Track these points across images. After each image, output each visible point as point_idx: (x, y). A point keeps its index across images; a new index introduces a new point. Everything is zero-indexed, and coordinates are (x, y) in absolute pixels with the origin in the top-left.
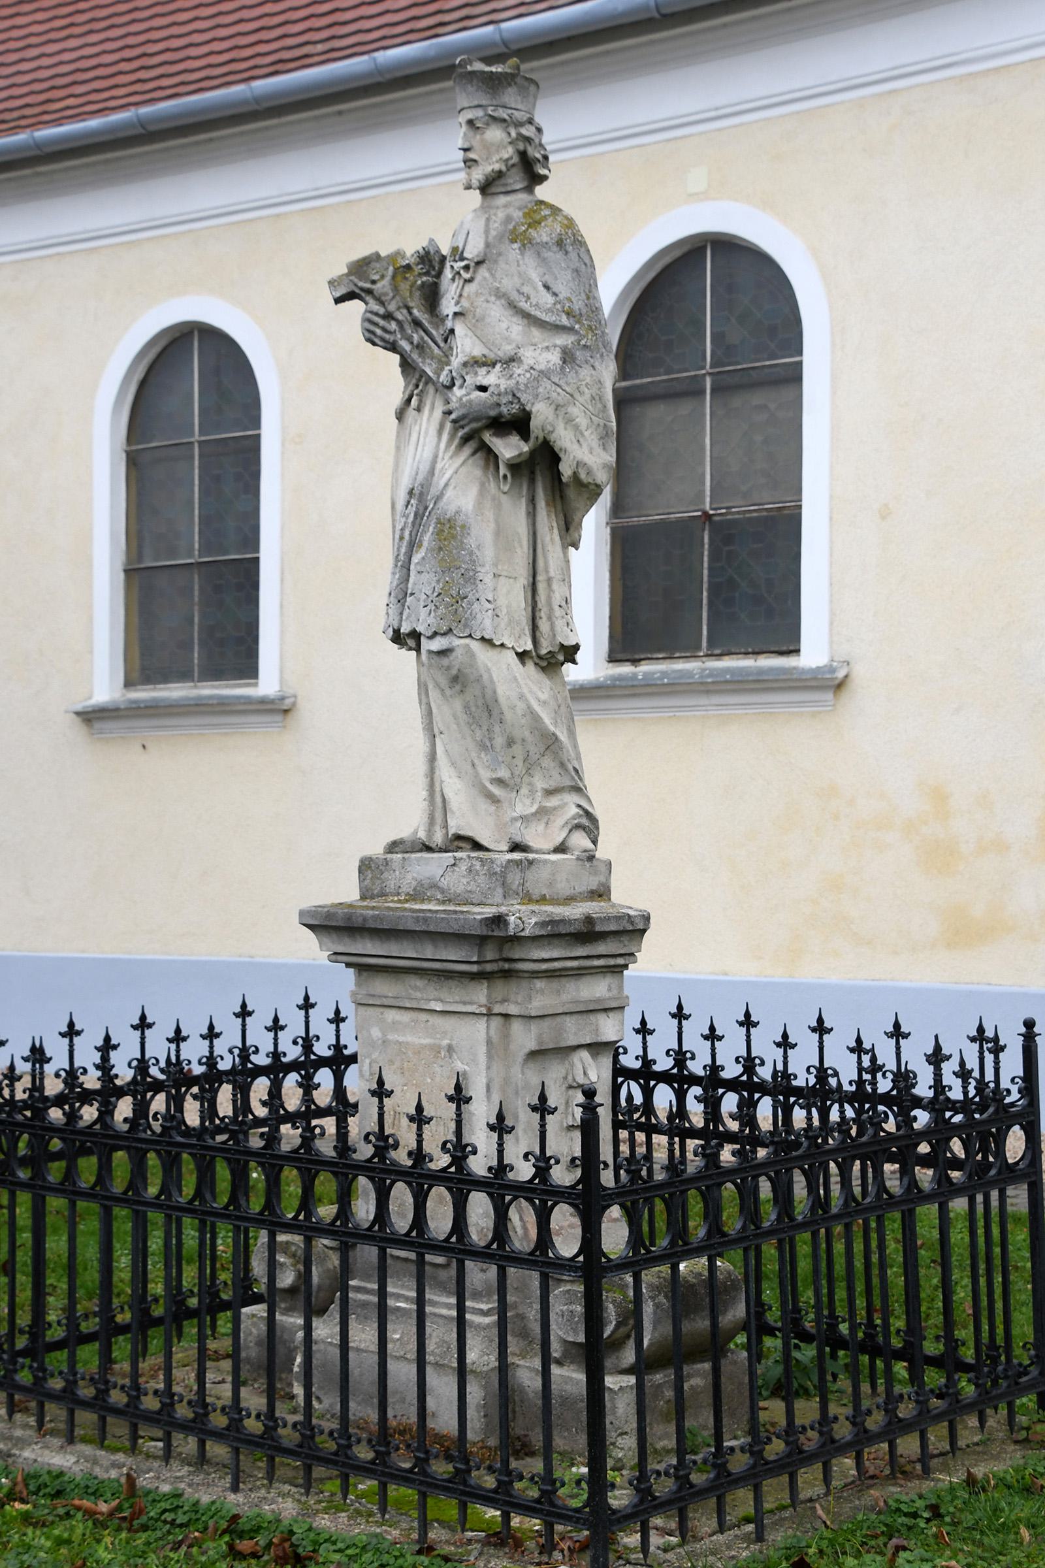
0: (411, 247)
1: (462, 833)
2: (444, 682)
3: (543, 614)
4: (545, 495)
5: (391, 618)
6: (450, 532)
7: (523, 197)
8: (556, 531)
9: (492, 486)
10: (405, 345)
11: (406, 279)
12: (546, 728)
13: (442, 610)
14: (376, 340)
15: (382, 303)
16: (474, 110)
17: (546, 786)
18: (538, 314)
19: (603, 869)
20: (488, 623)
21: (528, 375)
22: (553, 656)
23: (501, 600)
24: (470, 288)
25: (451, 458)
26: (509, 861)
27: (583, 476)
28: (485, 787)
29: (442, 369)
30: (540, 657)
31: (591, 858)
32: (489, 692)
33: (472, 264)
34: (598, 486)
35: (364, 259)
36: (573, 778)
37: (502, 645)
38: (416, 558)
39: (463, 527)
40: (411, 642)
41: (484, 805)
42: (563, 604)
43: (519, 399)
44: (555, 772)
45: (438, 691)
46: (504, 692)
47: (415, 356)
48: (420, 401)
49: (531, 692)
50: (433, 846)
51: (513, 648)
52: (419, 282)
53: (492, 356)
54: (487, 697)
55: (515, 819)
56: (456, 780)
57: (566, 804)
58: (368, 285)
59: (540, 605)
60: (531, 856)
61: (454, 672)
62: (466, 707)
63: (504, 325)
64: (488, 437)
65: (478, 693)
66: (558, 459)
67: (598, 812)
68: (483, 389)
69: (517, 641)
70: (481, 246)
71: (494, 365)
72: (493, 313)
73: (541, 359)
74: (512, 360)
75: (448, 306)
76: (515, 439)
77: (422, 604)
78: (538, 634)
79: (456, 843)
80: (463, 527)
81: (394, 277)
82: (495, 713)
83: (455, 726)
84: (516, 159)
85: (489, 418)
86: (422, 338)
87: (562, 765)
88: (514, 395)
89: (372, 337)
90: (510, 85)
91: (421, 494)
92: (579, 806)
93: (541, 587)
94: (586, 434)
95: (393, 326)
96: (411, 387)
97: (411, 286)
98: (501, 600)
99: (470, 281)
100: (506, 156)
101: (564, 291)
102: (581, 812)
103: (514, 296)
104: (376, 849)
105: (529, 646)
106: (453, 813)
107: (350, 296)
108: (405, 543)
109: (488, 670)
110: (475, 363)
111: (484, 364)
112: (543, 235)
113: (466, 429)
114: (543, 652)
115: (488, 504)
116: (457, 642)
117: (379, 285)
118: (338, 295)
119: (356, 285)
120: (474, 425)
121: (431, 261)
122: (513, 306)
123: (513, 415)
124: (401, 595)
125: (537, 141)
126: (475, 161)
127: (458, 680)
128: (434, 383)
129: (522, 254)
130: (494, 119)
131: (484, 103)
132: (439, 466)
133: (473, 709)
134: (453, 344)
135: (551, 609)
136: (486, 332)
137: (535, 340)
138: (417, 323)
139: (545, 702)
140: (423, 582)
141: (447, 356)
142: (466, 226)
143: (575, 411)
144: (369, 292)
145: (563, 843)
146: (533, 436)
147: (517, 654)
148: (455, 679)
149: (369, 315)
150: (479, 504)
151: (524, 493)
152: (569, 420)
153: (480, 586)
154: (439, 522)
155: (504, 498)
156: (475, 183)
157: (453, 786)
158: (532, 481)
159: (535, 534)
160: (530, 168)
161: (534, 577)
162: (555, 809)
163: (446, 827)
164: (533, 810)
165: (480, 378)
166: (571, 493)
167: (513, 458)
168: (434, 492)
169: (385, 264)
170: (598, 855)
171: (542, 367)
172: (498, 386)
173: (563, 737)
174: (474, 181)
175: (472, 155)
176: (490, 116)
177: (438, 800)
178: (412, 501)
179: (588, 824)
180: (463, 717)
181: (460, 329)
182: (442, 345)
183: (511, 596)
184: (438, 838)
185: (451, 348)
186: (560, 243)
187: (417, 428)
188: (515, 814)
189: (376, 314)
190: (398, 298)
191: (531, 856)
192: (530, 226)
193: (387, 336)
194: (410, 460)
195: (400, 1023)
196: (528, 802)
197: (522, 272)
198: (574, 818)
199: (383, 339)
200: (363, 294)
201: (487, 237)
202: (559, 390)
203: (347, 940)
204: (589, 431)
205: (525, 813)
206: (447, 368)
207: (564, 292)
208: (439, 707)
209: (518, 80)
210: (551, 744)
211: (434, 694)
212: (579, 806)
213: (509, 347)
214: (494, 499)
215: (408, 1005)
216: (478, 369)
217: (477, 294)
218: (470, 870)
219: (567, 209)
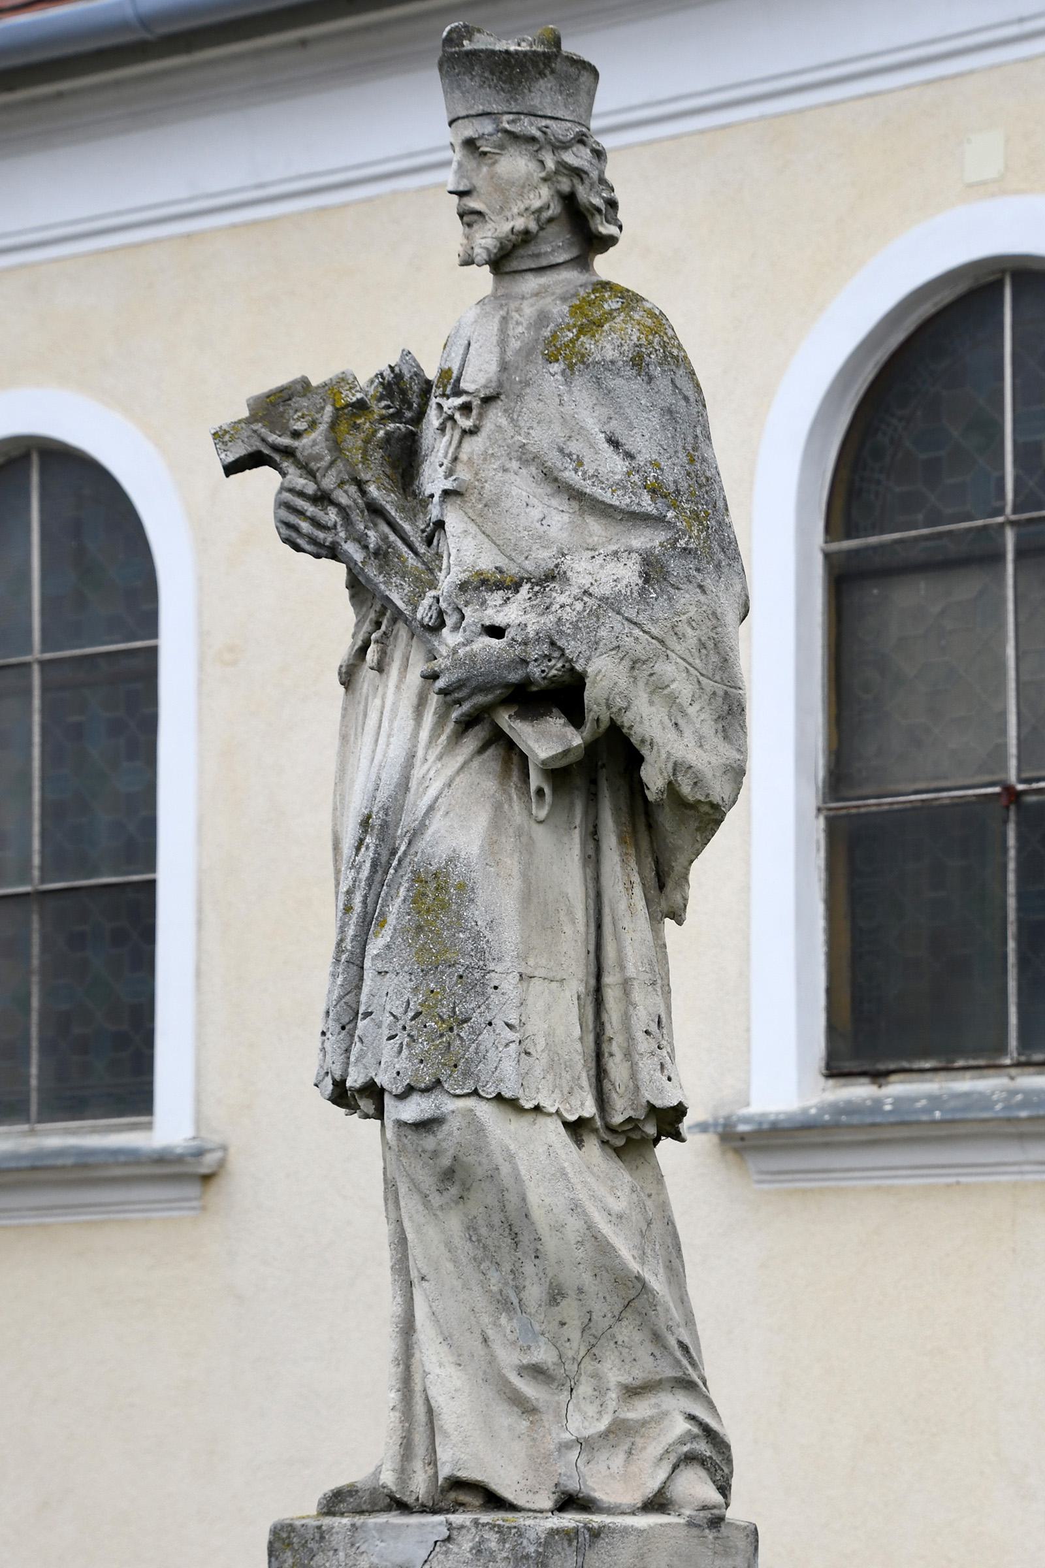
0: (366, 367)
1: (463, 1474)
2: (427, 1181)
3: (615, 1048)
4: (617, 823)
5: (329, 1059)
6: (438, 896)
7: (571, 277)
8: (638, 891)
9: (516, 810)
10: (352, 549)
11: (357, 427)
12: (624, 1267)
13: (422, 1045)
14: (301, 542)
15: (311, 474)
16: (476, 122)
17: (626, 1379)
18: (597, 492)
19: (742, 1543)
20: (508, 1067)
21: (579, 606)
22: (636, 1128)
23: (534, 1023)
24: (473, 446)
25: (440, 758)
26: (553, 1532)
27: (686, 789)
28: (507, 1382)
29: (421, 596)
30: (611, 1129)
31: (716, 1522)
32: (512, 1198)
33: (476, 402)
34: (715, 807)
35: (281, 390)
36: (678, 1362)
37: (537, 1109)
38: (373, 948)
39: (461, 887)
40: (366, 1105)
41: (507, 1419)
42: (653, 1028)
43: (562, 650)
44: (643, 1352)
45: (416, 1197)
46: (542, 1199)
47: (371, 571)
48: (383, 654)
49: (593, 1197)
50: (410, 1500)
51: (557, 1112)
52: (381, 433)
53: (513, 570)
54: (510, 1207)
55: (565, 1446)
56: (452, 1370)
57: (665, 1414)
58: (285, 441)
59: (609, 1032)
60: (596, 1520)
61: (446, 1162)
62: (471, 1228)
63: (536, 513)
64: (505, 720)
65: (491, 1200)
66: (639, 759)
67: (730, 1430)
68: (496, 632)
69: (565, 1100)
70: (493, 368)
71: (516, 587)
72: (515, 491)
73: (603, 575)
74: (551, 577)
75: (433, 480)
76: (556, 724)
77: (386, 1033)
78: (607, 1085)
79: (452, 1495)
80: (461, 887)
81: (333, 425)
82: (525, 1239)
83: (450, 1266)
84: (555, 209)
85: (508, 685)
86: (385, 538)
87: (657, 1337)
88: (553, 644)
89: (294, 535)
90: (542, 74)
91: (385, 825)
92: (692, 1418)
93: (612, 996)
94: (692, 710)
95: (332, 516)
96: (367, 626)
97: (367, 442)
98: (534, 1023)
99: (473, 432)
100: (537, 204)
101: (645, 446)
102: (696, 1430)
103: (553, 459)
104: (302, 1507)
105: (589, 1109)
106: (446, 1435)
107: (253, 460)
108: (354, 917)
109: (511, 1158)
110: (482, 584)
111: (499, 586)
112: (606, 347)
113: (466, 707)
114: (617, 1119)
115: (508, 843)
116: (450, 1105)
117: (305, 441)
118: (231, 458)
119: (263, 440)
120: (480, 699)
121: (405, 393)
122: (550, 477)
123: (552, 680)
124: (348, 1016)
125: (594, 175)
127: (454, 1177)
128: (406, 621)
129: (568, 383)
130: (514, 137)
131: (495, 108)
132: (417, 773)
133: (484, 1231)
134: (443, 548)
135: (630, 1038)
136: (505, 524)
137: (592, 541)
138: (375, 511)
139: (620, 1217)
140: (388, 992)
141: (431, 571)
142: (466, 332)
143: (667, 669)
144: (288, 452)
145: (661, 1492)
146: (589, 717)
147: (566, 1124)
148: (448, 1176)
149: (287, 496)
150: (491, 845)
151: (578, 821)
152: (658, 688)
153: (495, 998)
154: (416, 878)
155: (539, 832)
156: (480, 254)
157: (447, 1382)
158: (593, 798)
159: (598, 896)
160: (583, 225)
161: (599, 976)
162: (644, 1423)
163: (433, 1462)
164: (602, 1426)
165: (490, 611)
166: (666, 820)
167: (554, 758)
168: (408, 821)
169: (319, 400)
170: (730, 1514)
171: (605, 590)
172: (523, 626)
173: (657, 1283)
174: (477, 250)
175: (473, 204)
176: (506, 131)
177: (420, 1409)
178: (368, 840)
179: (711, 1453)
180: (465, 1249)
181: (454, 521)
182: (422, 549)
183: (553, 1015)
184: (420, 1486)
185: (439, 556)
186: (638, 362)
187: (378, 702)
188: (566, 1436)
189: (301, 494)
190: (340, 464)
191: (596, 1520)
192: (582, 330)
193: (321, 535)
194: (364, 763)
196: (591, 1410)
197: (568, 414)
198: (681, 1441)
199: (313, 541)
200: (277, 457)
201: (503, 352)
202: (637, 632)
204: (696, 707)
205: (586, 1433)
206: (433, 593)
207: (646, 451)
208: (418, 1230)
209: (558, 65)
210: (633, 1296)
211: (410, 1204)
212: (692, 1418)
213: (545, 554)
214: (519, 834)
216: (487, 595)
217: (486, 457)
219: (656, 296)
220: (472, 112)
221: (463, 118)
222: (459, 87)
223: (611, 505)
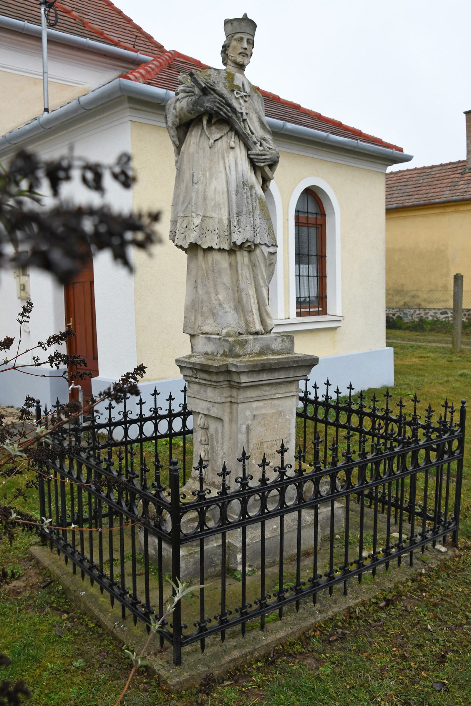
126: (247, 55)
189: (222, 101)
195: (259, 406)
203: (255, 375)
215: (266, 398)
218: (283, 340)
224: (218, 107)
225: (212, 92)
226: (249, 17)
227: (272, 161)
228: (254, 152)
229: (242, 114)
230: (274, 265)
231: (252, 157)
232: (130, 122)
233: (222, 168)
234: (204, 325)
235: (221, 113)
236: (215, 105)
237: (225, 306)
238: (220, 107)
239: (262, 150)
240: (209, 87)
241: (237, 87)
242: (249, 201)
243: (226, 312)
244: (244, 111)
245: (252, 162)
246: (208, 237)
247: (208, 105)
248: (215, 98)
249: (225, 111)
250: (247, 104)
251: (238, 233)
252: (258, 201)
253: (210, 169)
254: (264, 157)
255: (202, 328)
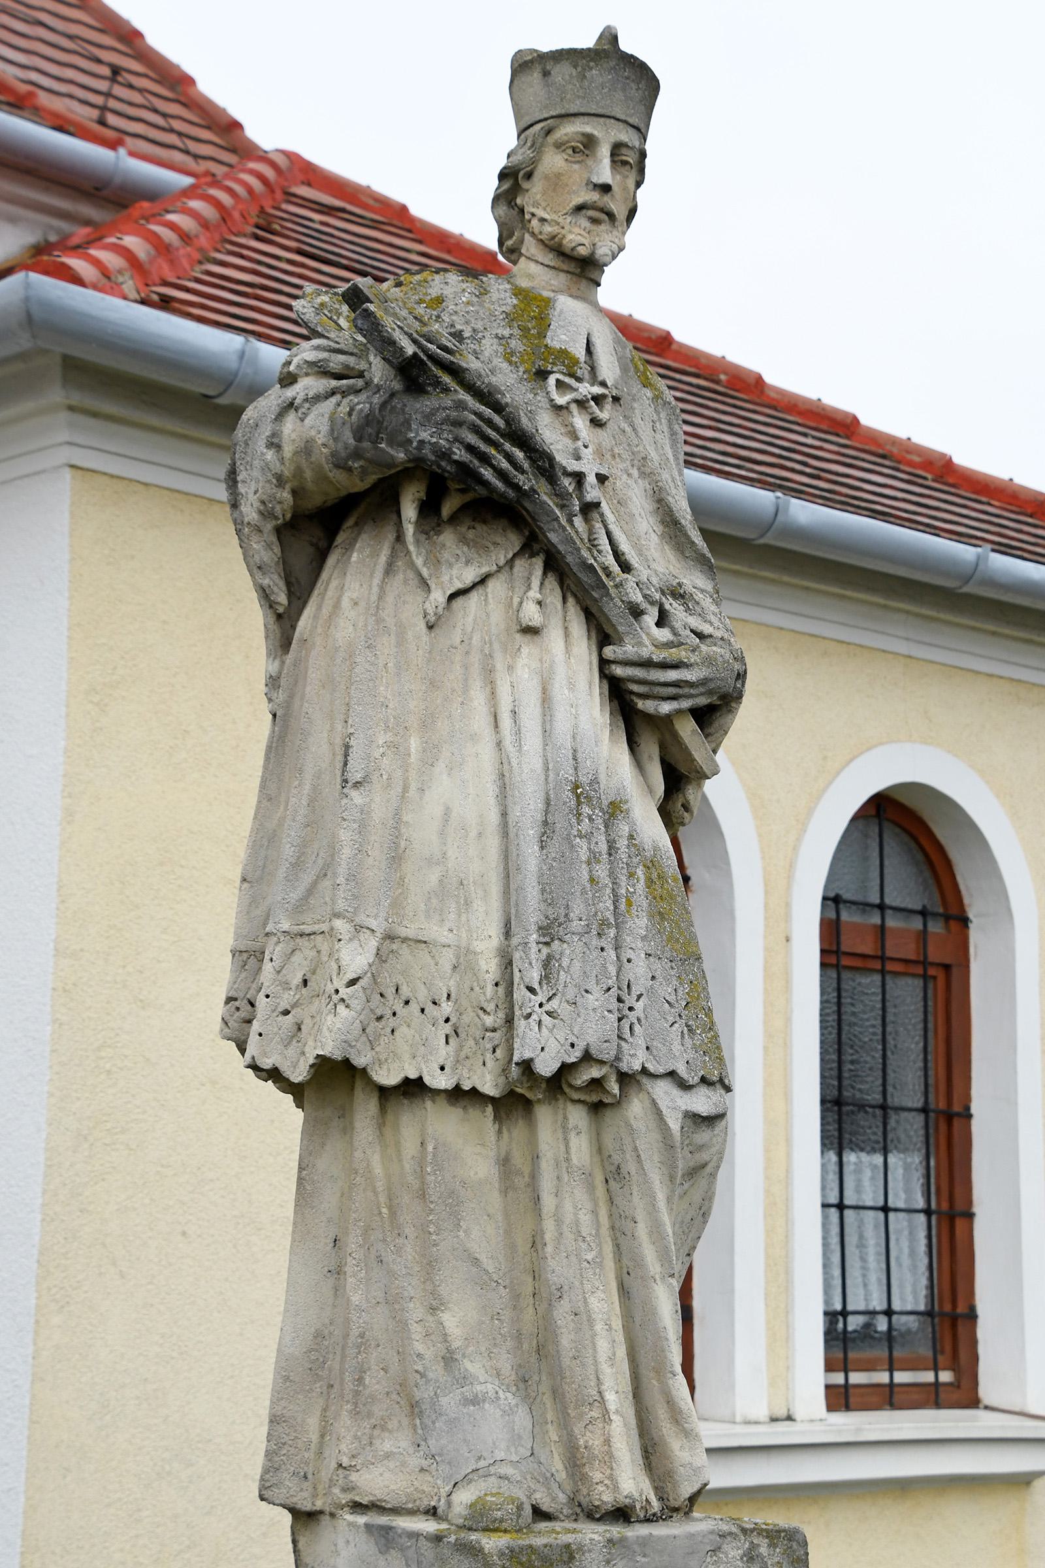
16: (631, 131)
72: (635, 499)
126: (611, 216)
189: (490, 423)
220: (631, 120)
221: (618, 120)
222: (624, 90)
223: (693, 542)
224: (470, 449)
225: (446, 379)
226: (625, 46)
227: (710, 693)
228: (628, 650)
229: (579, 478)
230: (713, 1175)
231: (619, 671)
232: (67, 474)
233: (480, 721)
234: (368, 1464)
235: (487, 473)
236: (457, 439)
237: (474, 1367)
238: (483, 447)
239: (669, 645)
240: (432, 357)
241: (563, 355)
242: (602, 872)
243: (475, 1401)
244: (589, 467)
245: (620, 697)
246: (403, 1031)
247: (424, 435)
248: (460, 405)
249: (505, 464)
250: (603, 437)
251: (545, 1018)
252: (640, 872)
253: (427, 724)
254: (672, 675)
255: (354, 1477)
